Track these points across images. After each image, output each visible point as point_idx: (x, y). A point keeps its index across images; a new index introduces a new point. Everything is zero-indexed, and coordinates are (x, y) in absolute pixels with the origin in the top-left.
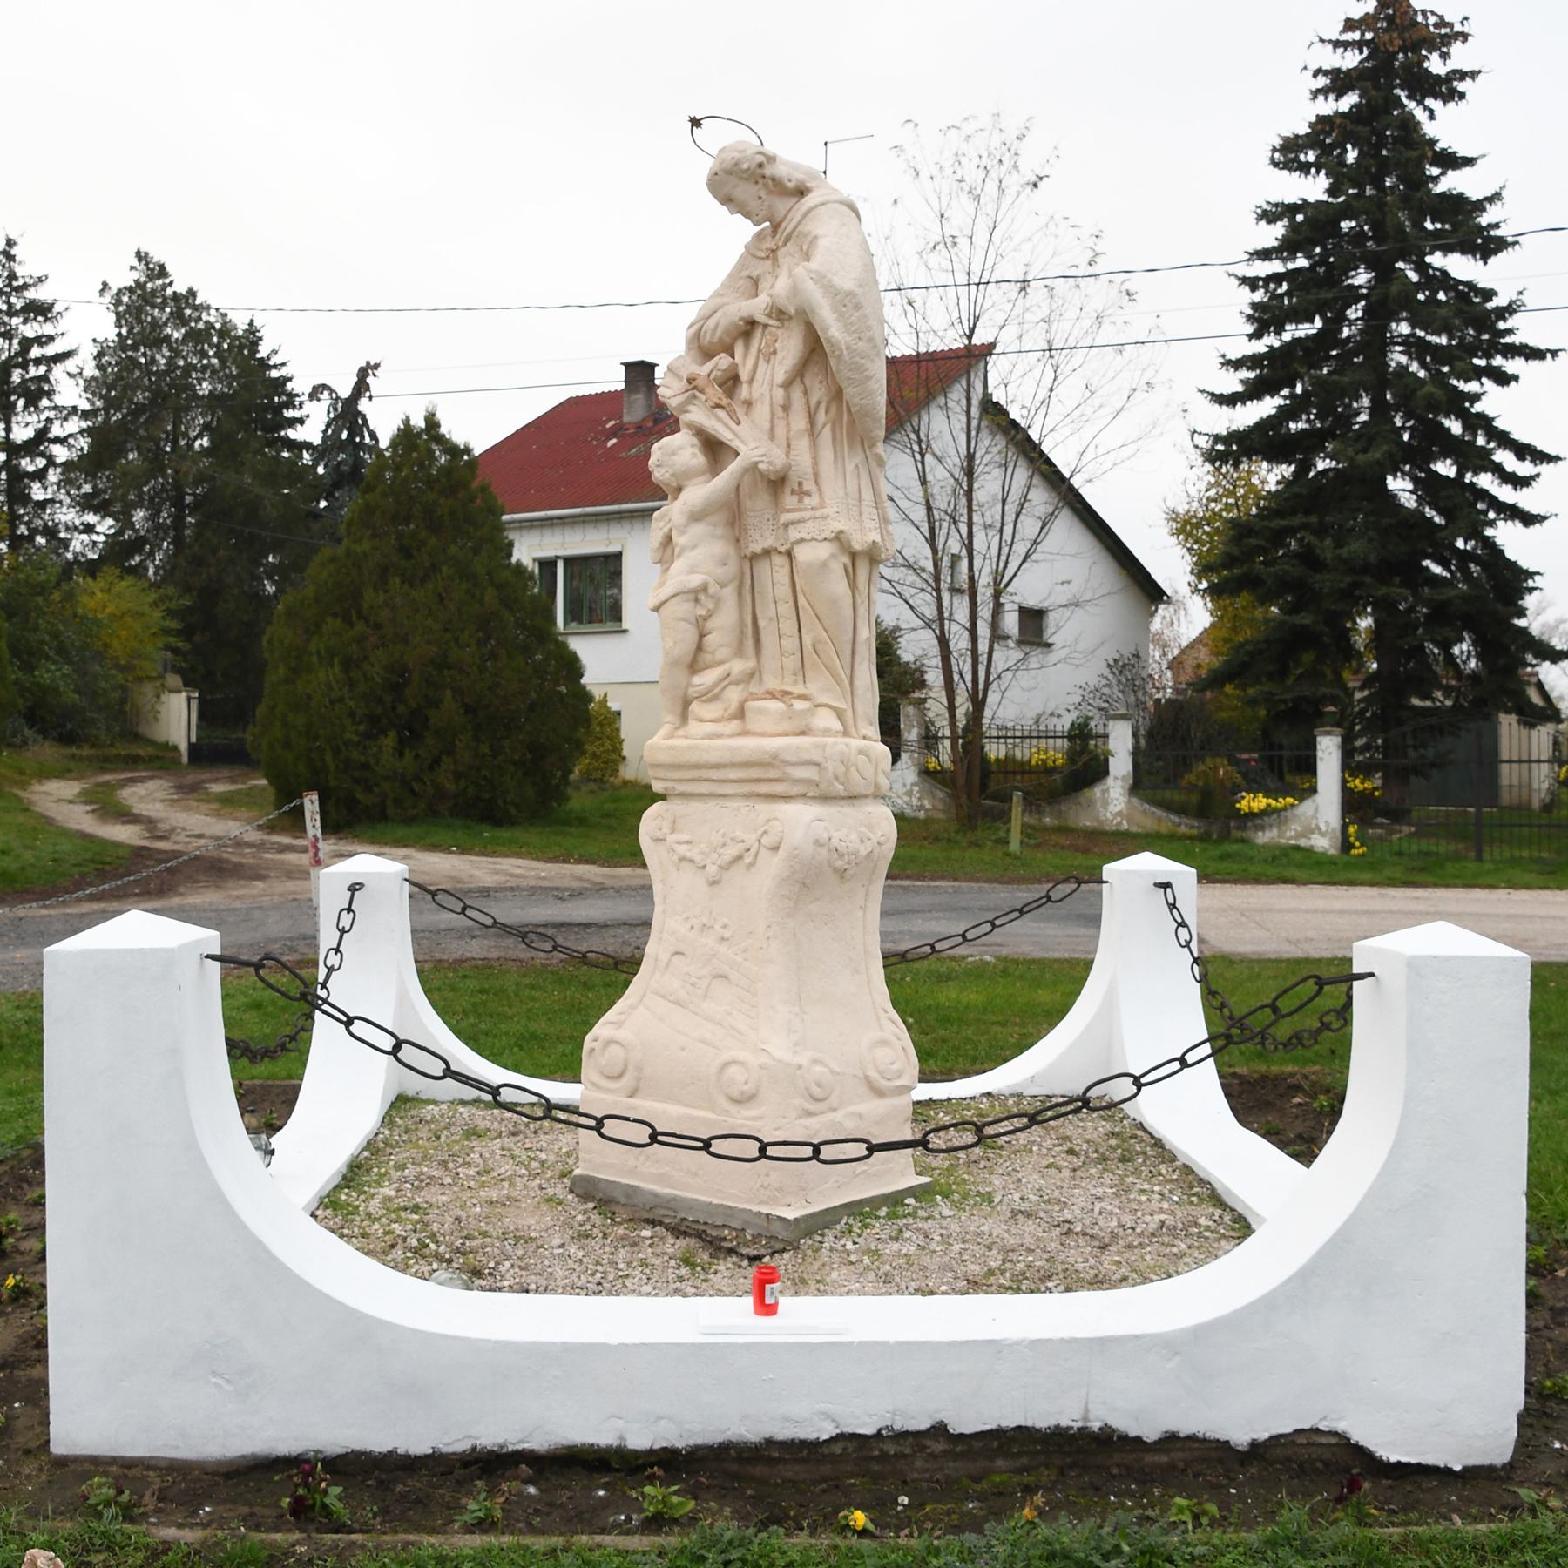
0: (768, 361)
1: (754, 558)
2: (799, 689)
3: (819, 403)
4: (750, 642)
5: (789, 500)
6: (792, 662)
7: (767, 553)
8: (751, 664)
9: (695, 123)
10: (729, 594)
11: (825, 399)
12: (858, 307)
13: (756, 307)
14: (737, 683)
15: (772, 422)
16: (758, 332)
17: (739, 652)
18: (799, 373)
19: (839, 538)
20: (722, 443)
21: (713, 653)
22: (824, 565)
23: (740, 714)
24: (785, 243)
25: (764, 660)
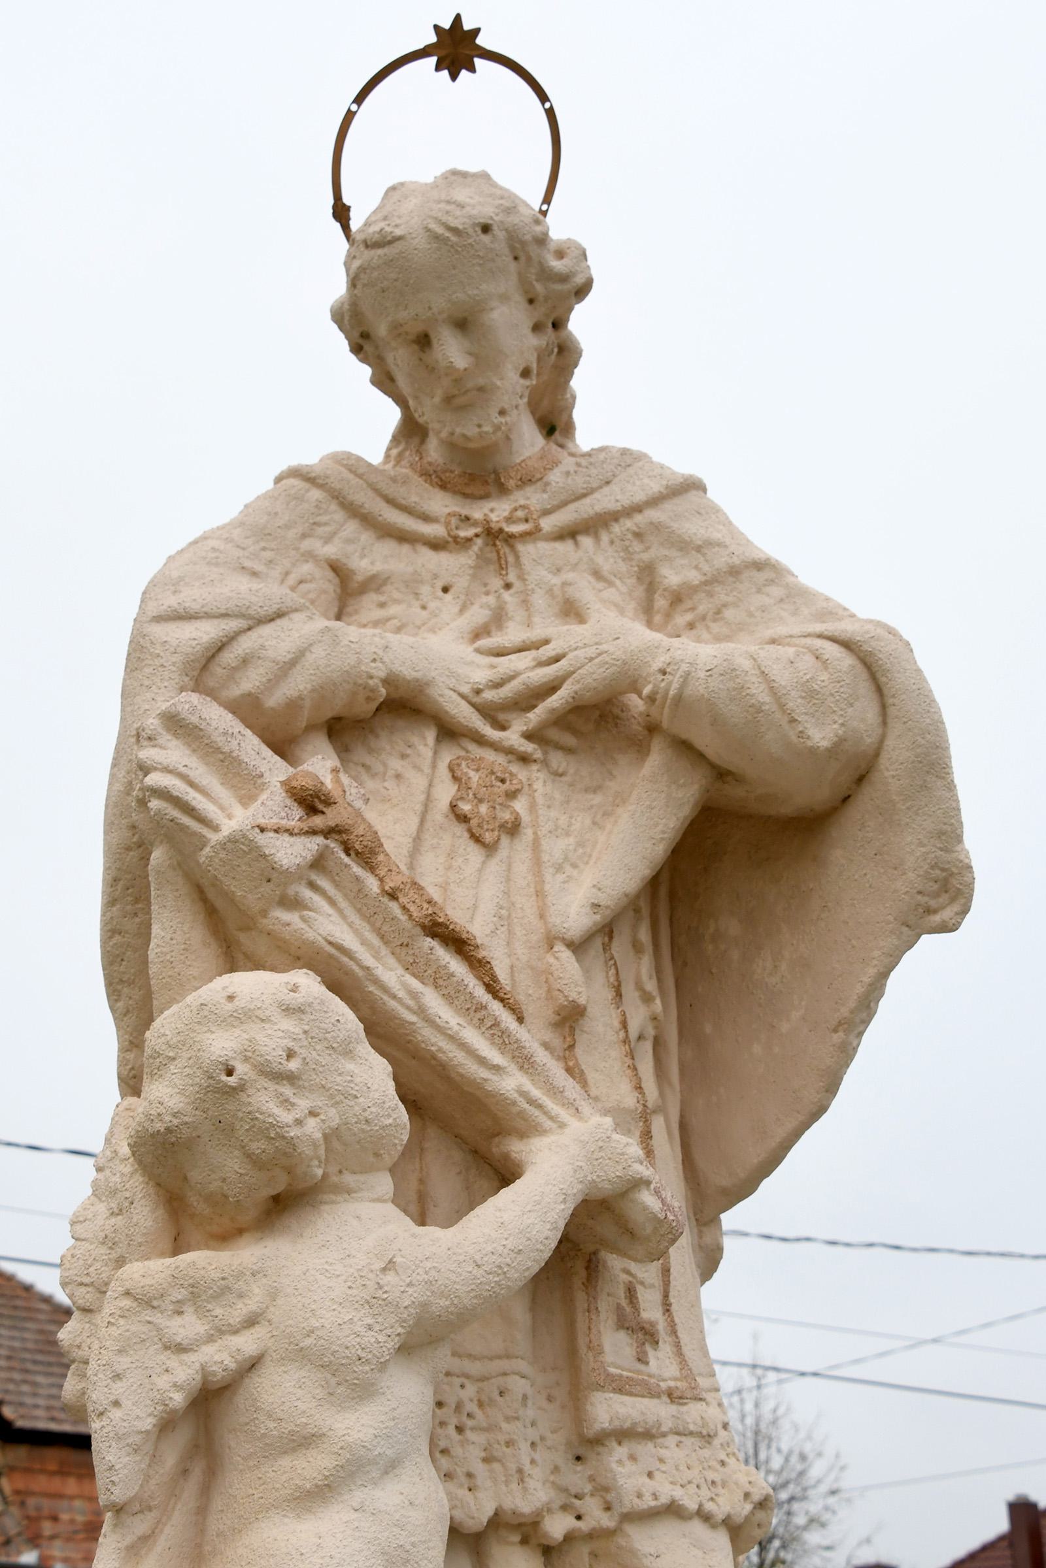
5: (615, 1349)
9: (456, 49)
24: (570, 534)
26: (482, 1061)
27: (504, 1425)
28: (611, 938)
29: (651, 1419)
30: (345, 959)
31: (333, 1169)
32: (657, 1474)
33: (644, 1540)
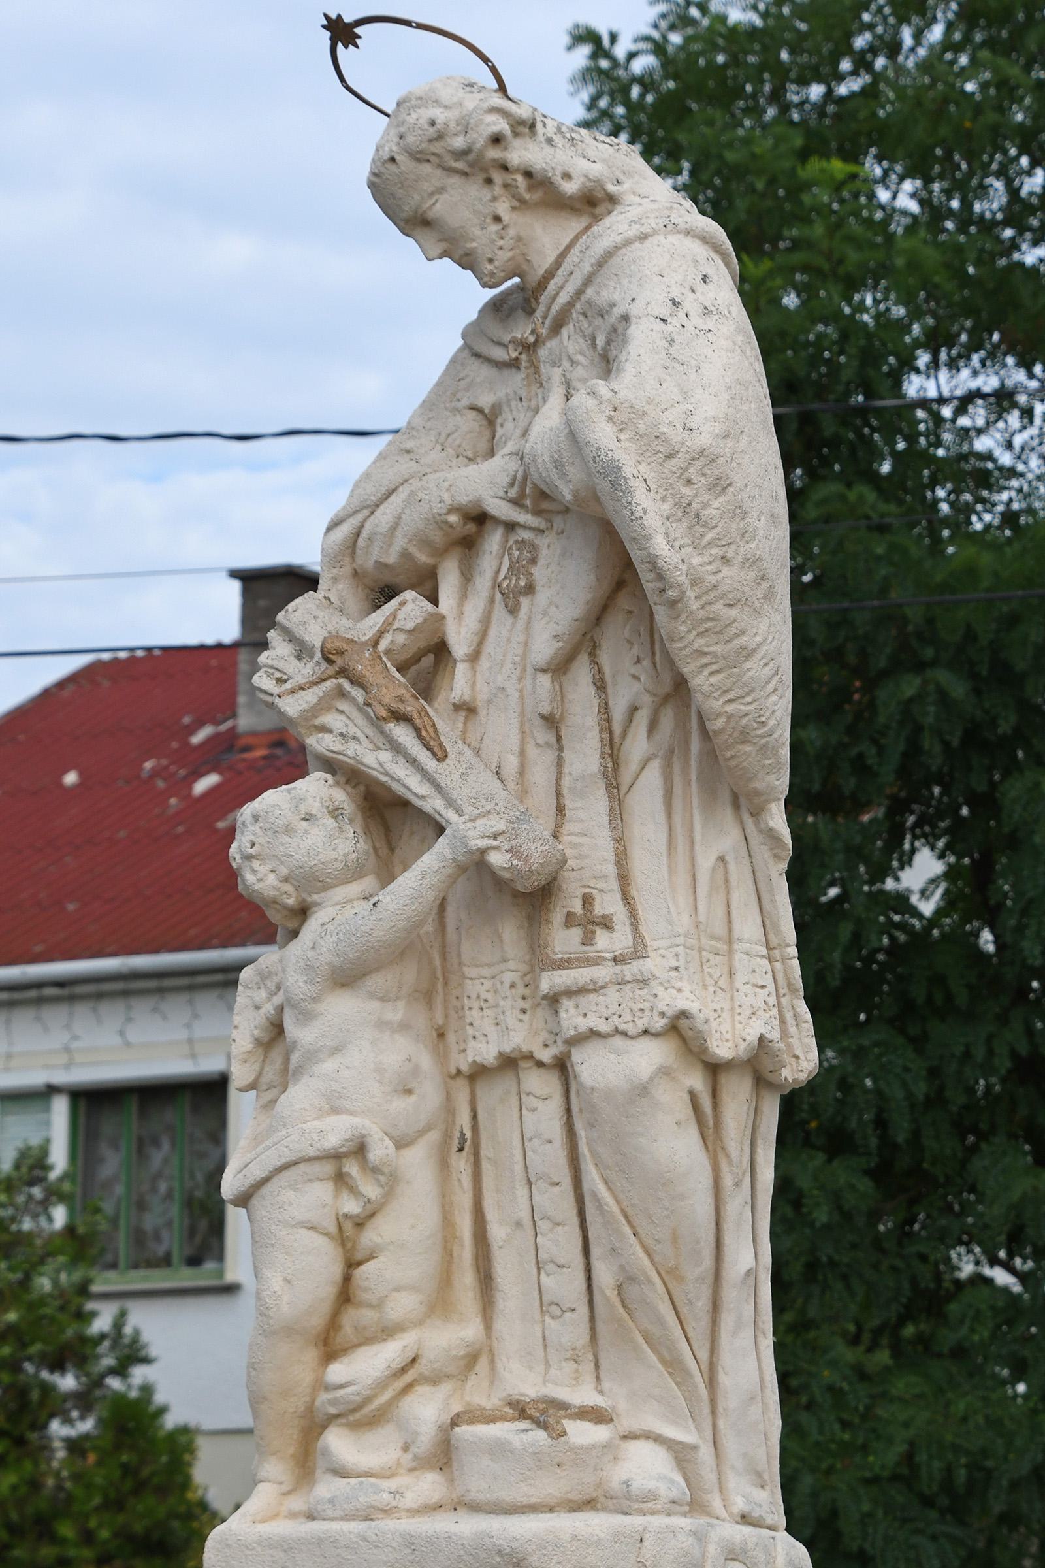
0: (513, 611)
1: (478, 1074)
2: (585, 1395)
3: (633, 709)
4: (466, 1279)
5: (563, 940)
6: (571, 1330)
7: (510, 1063)
8: (470, 1330)
9: (342, 32)
10: (417, 1164)
11: (647, 699)
12: (720, 485)
13: (484, 482)
14: (434, 1380)
15: (522, 753)
16: (494, 541)
17: (440, 1303)
18: (584, 642)
19: (679, 1030)
20: (404, 804)
21: (379, 1305)
22: (642, 1091)
23: (443, 1455)
24: (557, 327)
25: (499, 1325)
26: (414, 794)
27: (502, 1003)
28: (594, 647)
29: (581, 983)
30: (340, 757)
31: (304, 895)
32: (589, 1014)
33: (577, 1056)
